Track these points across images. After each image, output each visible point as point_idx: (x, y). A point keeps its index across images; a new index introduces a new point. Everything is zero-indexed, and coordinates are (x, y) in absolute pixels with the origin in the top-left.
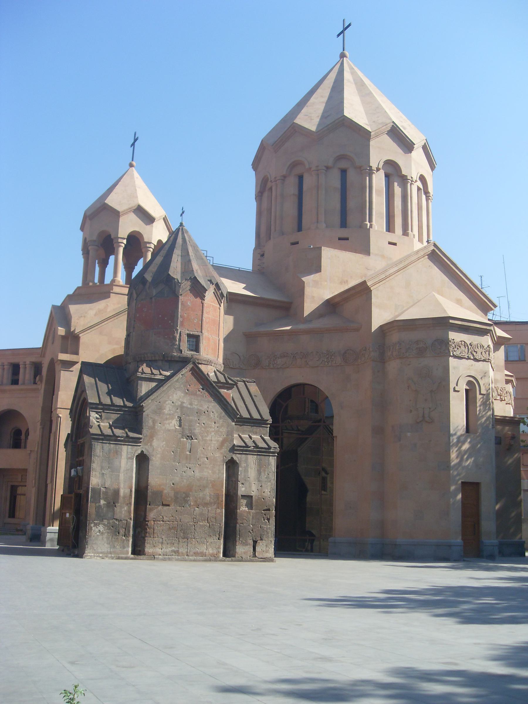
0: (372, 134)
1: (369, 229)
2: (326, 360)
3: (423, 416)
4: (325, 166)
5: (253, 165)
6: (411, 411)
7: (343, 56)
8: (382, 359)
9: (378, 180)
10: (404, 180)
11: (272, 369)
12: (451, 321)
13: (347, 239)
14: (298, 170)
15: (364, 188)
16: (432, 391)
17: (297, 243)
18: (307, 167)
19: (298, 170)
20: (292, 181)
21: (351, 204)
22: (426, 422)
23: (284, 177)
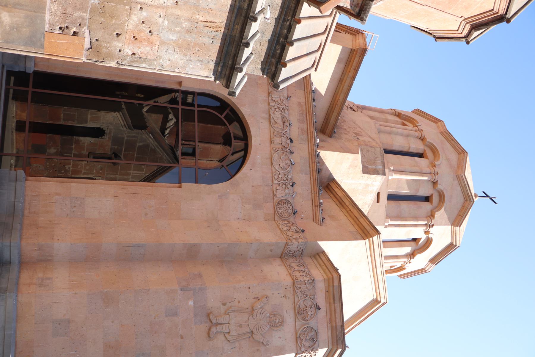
0: (458, 228)
1: (384, 225)
2: (280, 176)
3: (217, 324)
4: (437, 181)
5: (418, 110)
6: (224, 304)
8: (286, 255)
9: (419, 233)
10: (412, 255)
11: (269, 104)
12: (339, 351)
13: (378, 202)
14: (429, 153)
15: (416, 218)
16: (252, 333)
18: (437, 163)
19: (429, 153)
21: (404, 205)
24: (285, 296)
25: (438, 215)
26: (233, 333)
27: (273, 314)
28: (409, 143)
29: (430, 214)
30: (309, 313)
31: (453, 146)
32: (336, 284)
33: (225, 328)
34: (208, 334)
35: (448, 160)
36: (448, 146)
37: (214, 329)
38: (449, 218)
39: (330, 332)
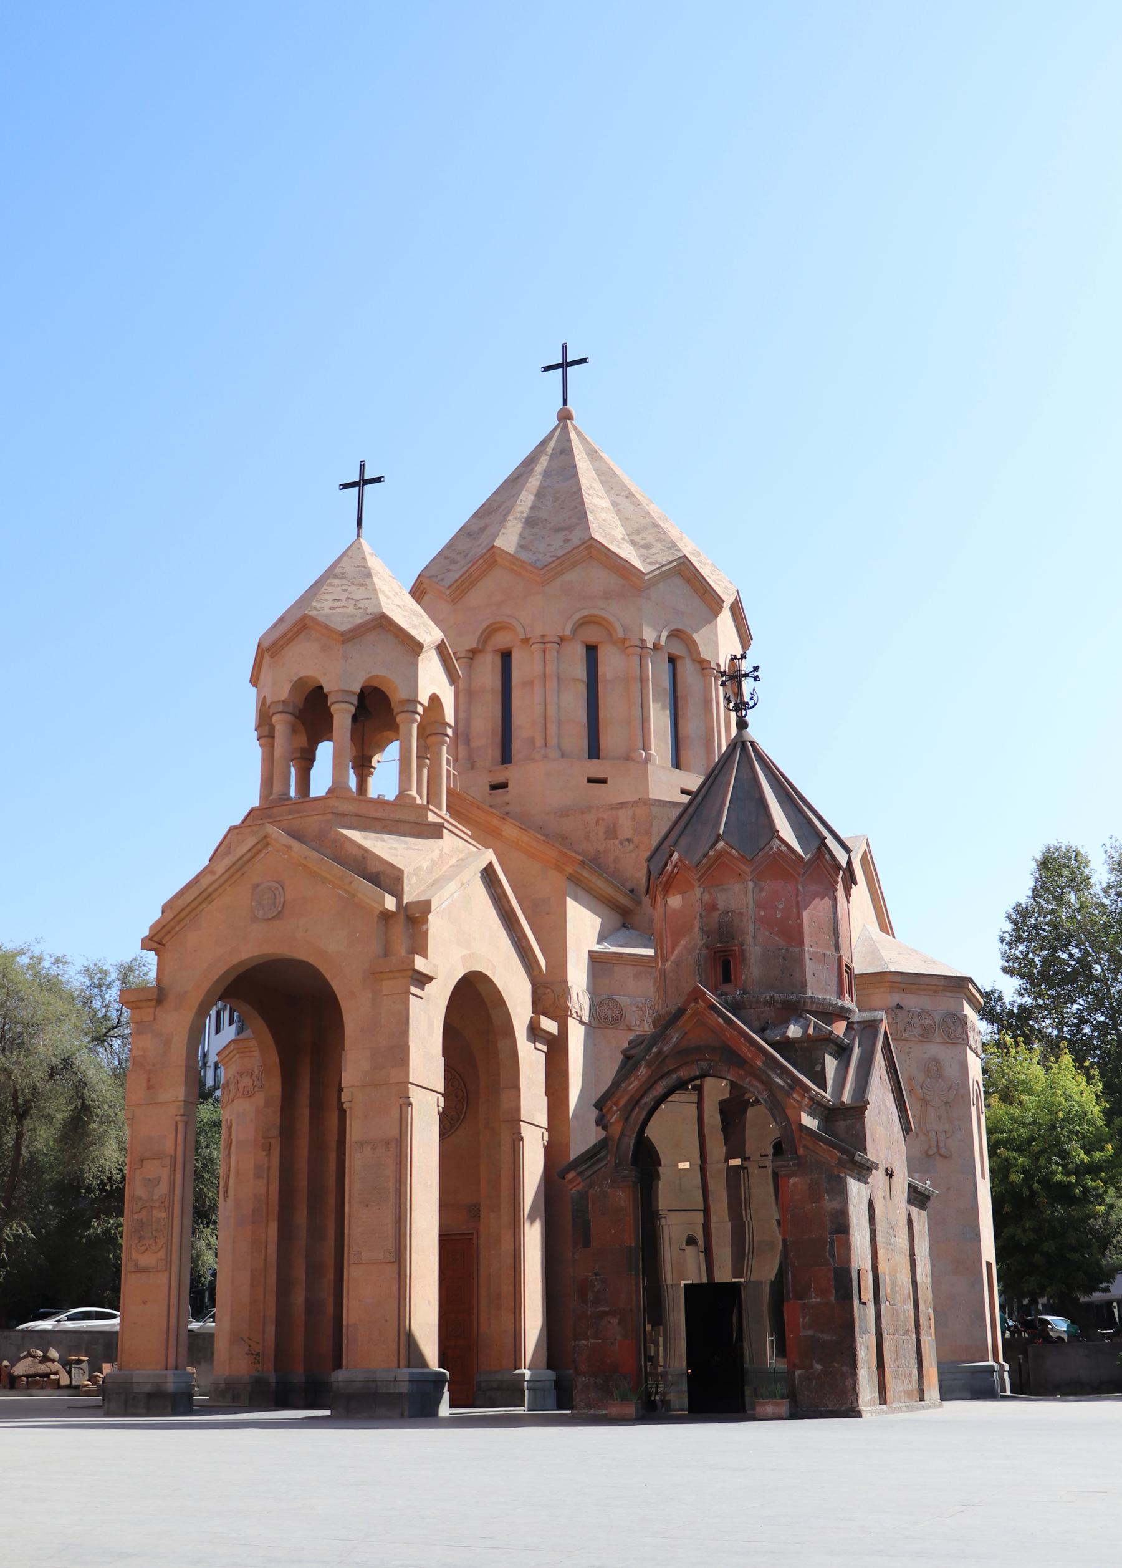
3: (938, 1147)
7: (565, 416)
12: (970, 986)
16: (946, 1103)
17: (604, 781)
19: (592, 635)
20: (578, 652)
22: (941, 1155)
23: (562, 640)
24: (909, 1053)
25: (705, 654)
26: (947, 1127)
27: (927, 1071)
28: (574, 680)
29: (698, 666)
30: (928, 1021)
31: (574, 565)
32: (898, 979)
33: (942, 1137)
34: (946, 1157)
35: (607, 596)
36: (569, 577)
37: (943, 1151)
38: (710, 622)
39: (948, 994)
